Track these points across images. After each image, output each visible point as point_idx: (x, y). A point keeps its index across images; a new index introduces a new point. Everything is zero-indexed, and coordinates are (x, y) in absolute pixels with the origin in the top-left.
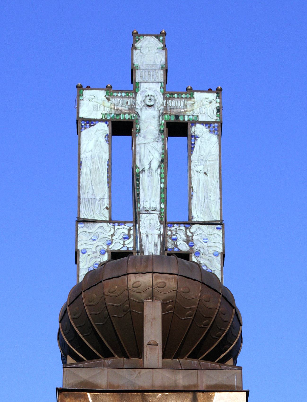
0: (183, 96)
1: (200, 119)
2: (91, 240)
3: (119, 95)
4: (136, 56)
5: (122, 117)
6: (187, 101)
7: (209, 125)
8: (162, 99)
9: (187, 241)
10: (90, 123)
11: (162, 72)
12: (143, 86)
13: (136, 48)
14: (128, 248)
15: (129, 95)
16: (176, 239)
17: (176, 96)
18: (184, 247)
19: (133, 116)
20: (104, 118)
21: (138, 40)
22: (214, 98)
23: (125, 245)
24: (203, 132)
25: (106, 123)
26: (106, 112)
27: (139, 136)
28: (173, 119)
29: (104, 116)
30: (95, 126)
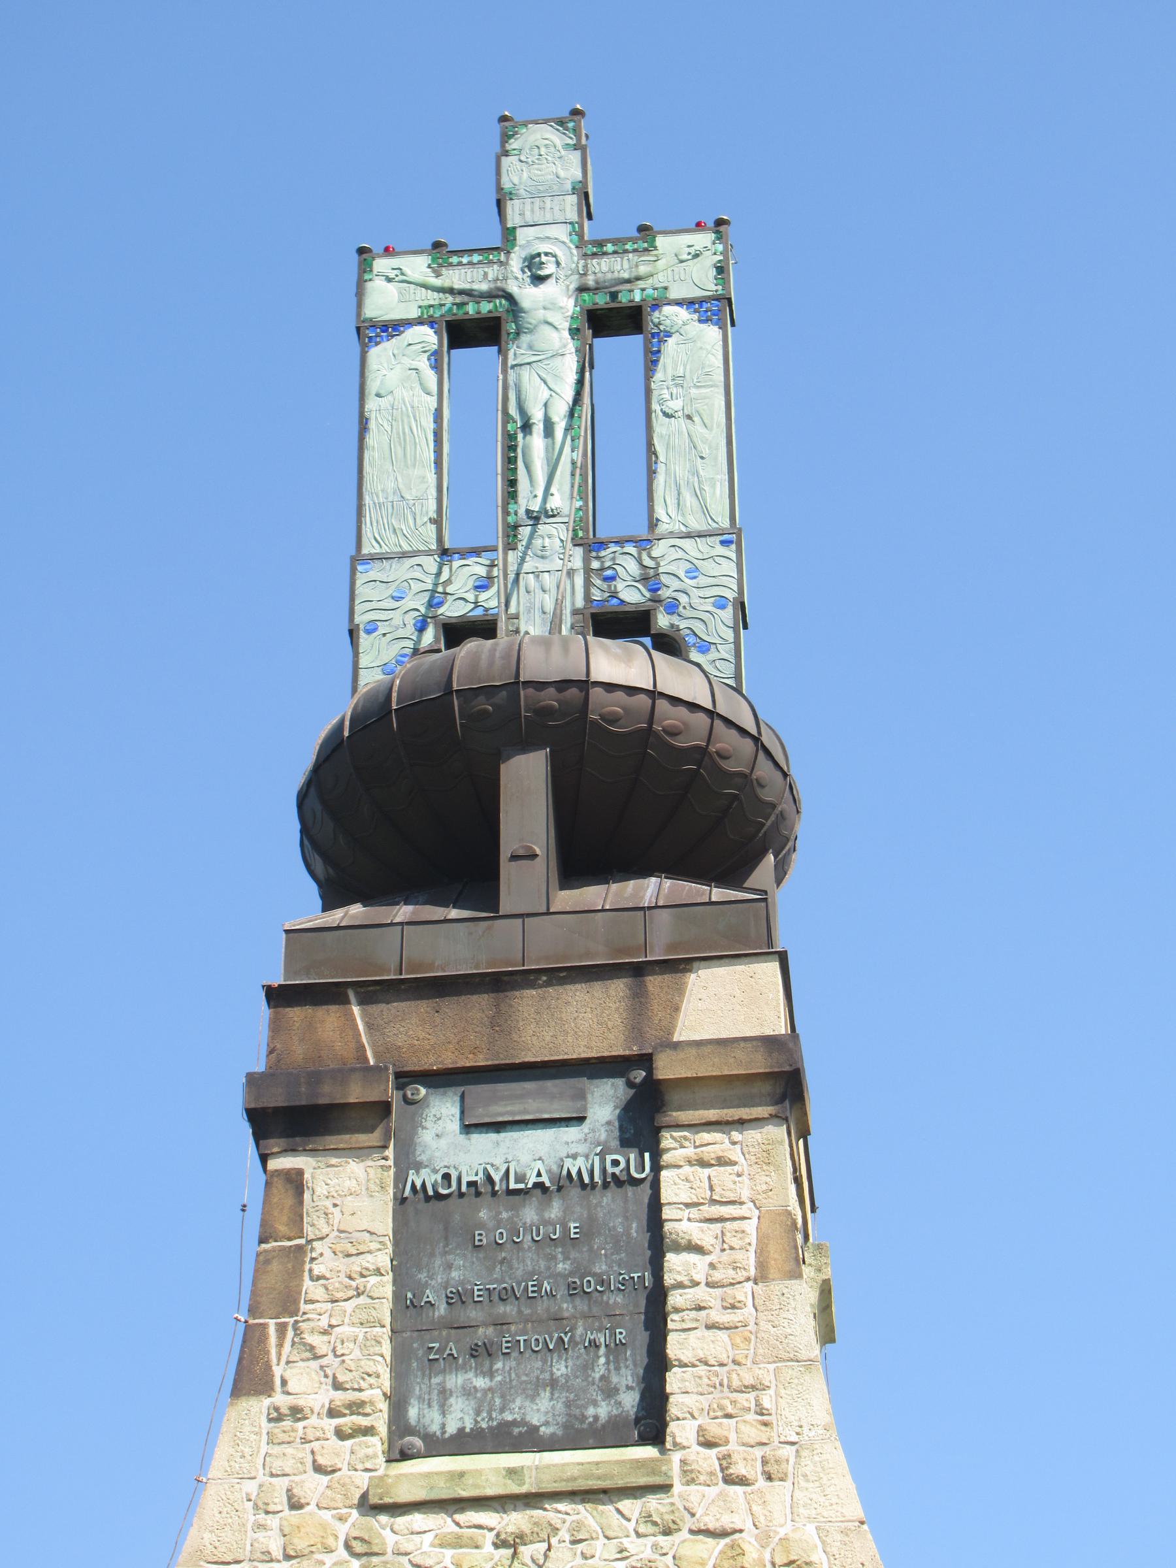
0: (629, 246)
1: (673, 294)
2: (390, 600)
3: (465, 260)
4: (508, 171)
5: (471, 309)
6: (640, 256)
7: (697, 306)
8: (576, 259)
9: (644, 579)
10: (390, 330)
11: (573, 199)
12: (522, 236)
13: (506, 153)
14: (486, 610)
15: (491, 257)
16: (612, 578)
17: (610, 248)
18: (632, 596)
19: (500, 303)
20: (425, 316)
21: (514, 135)
22: (709, 245)
23: (479, 604)
24: (681, 322)
25: (432, 327)
26: (432, 303)
27: (515, 346)
28: (602, 300)
29: (425, 311)
30: (403, 335)
